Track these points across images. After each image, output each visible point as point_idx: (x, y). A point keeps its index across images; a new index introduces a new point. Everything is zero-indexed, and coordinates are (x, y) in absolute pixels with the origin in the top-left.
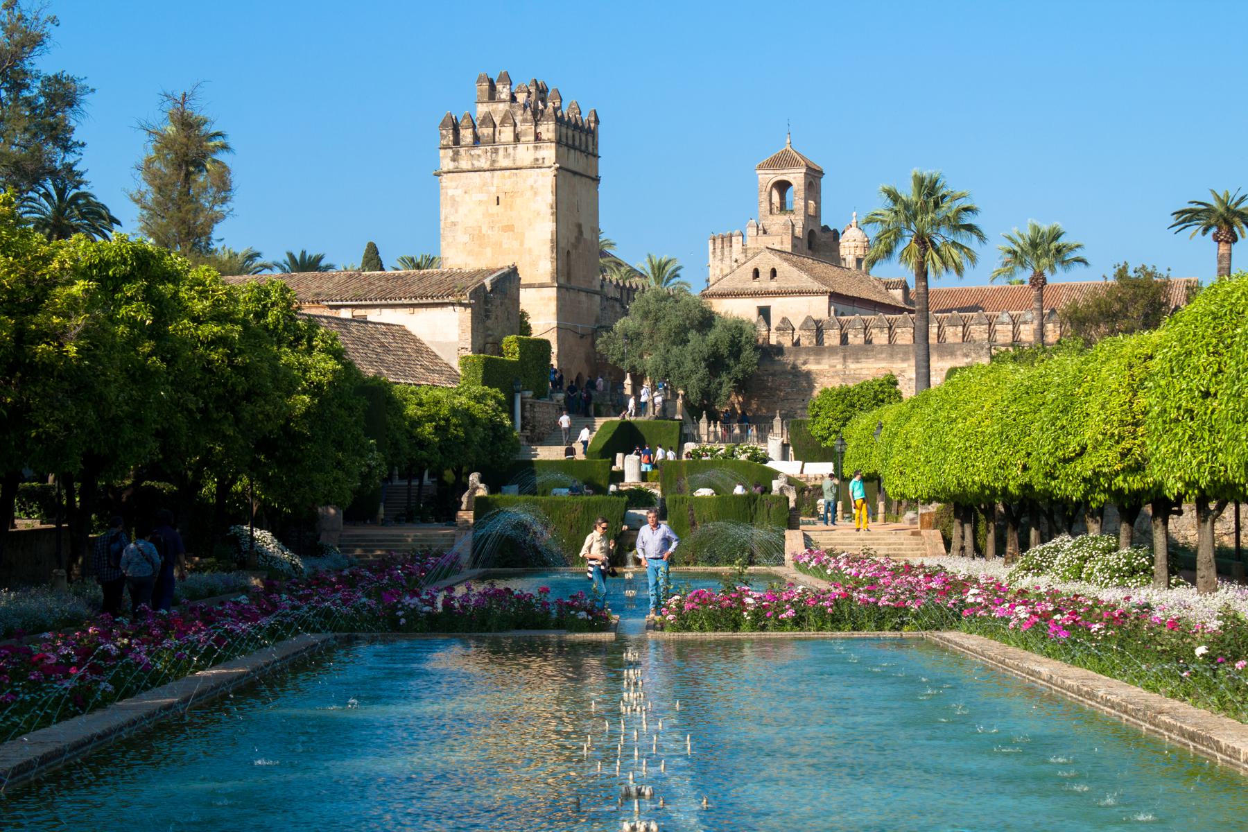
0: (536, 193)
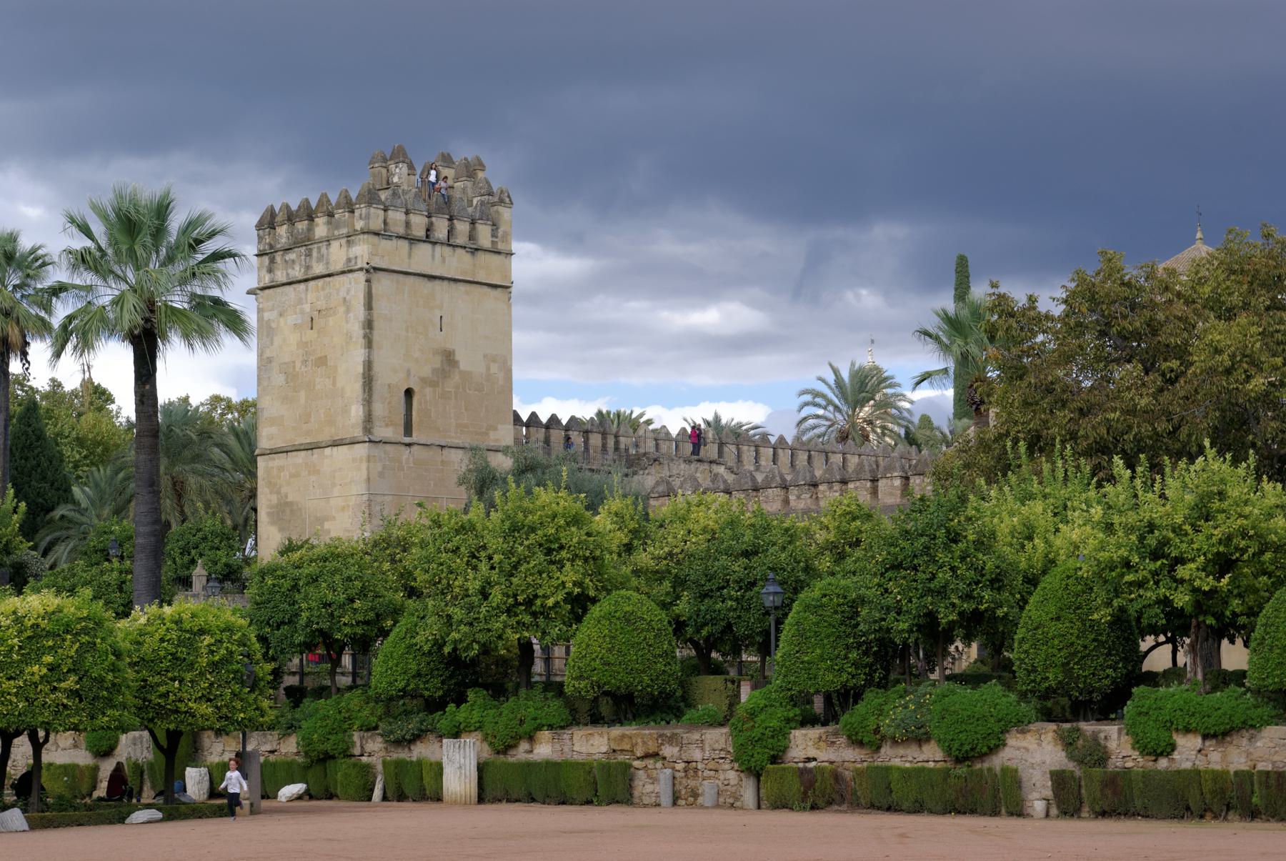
0: (348, 311)
